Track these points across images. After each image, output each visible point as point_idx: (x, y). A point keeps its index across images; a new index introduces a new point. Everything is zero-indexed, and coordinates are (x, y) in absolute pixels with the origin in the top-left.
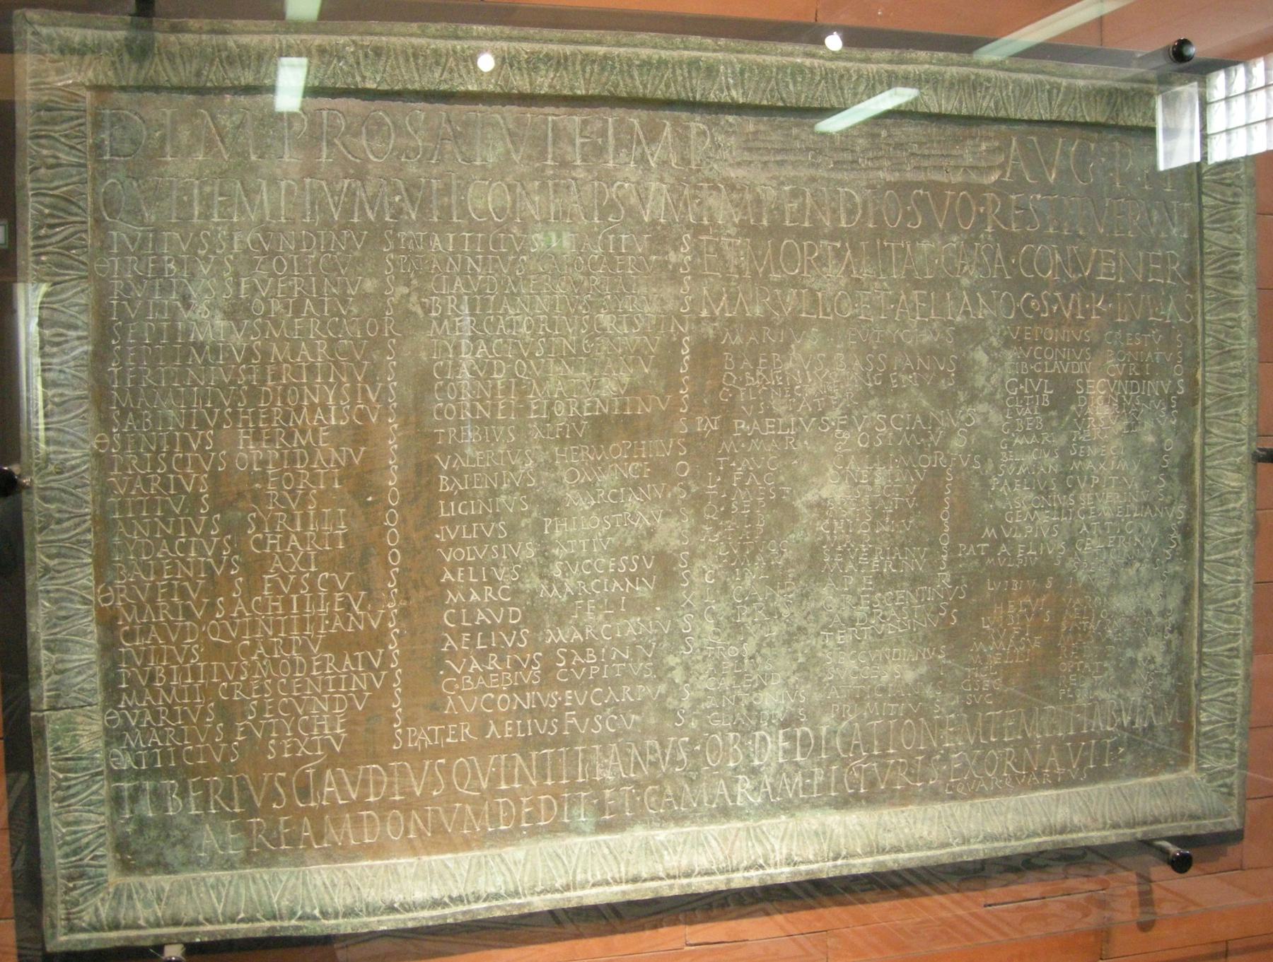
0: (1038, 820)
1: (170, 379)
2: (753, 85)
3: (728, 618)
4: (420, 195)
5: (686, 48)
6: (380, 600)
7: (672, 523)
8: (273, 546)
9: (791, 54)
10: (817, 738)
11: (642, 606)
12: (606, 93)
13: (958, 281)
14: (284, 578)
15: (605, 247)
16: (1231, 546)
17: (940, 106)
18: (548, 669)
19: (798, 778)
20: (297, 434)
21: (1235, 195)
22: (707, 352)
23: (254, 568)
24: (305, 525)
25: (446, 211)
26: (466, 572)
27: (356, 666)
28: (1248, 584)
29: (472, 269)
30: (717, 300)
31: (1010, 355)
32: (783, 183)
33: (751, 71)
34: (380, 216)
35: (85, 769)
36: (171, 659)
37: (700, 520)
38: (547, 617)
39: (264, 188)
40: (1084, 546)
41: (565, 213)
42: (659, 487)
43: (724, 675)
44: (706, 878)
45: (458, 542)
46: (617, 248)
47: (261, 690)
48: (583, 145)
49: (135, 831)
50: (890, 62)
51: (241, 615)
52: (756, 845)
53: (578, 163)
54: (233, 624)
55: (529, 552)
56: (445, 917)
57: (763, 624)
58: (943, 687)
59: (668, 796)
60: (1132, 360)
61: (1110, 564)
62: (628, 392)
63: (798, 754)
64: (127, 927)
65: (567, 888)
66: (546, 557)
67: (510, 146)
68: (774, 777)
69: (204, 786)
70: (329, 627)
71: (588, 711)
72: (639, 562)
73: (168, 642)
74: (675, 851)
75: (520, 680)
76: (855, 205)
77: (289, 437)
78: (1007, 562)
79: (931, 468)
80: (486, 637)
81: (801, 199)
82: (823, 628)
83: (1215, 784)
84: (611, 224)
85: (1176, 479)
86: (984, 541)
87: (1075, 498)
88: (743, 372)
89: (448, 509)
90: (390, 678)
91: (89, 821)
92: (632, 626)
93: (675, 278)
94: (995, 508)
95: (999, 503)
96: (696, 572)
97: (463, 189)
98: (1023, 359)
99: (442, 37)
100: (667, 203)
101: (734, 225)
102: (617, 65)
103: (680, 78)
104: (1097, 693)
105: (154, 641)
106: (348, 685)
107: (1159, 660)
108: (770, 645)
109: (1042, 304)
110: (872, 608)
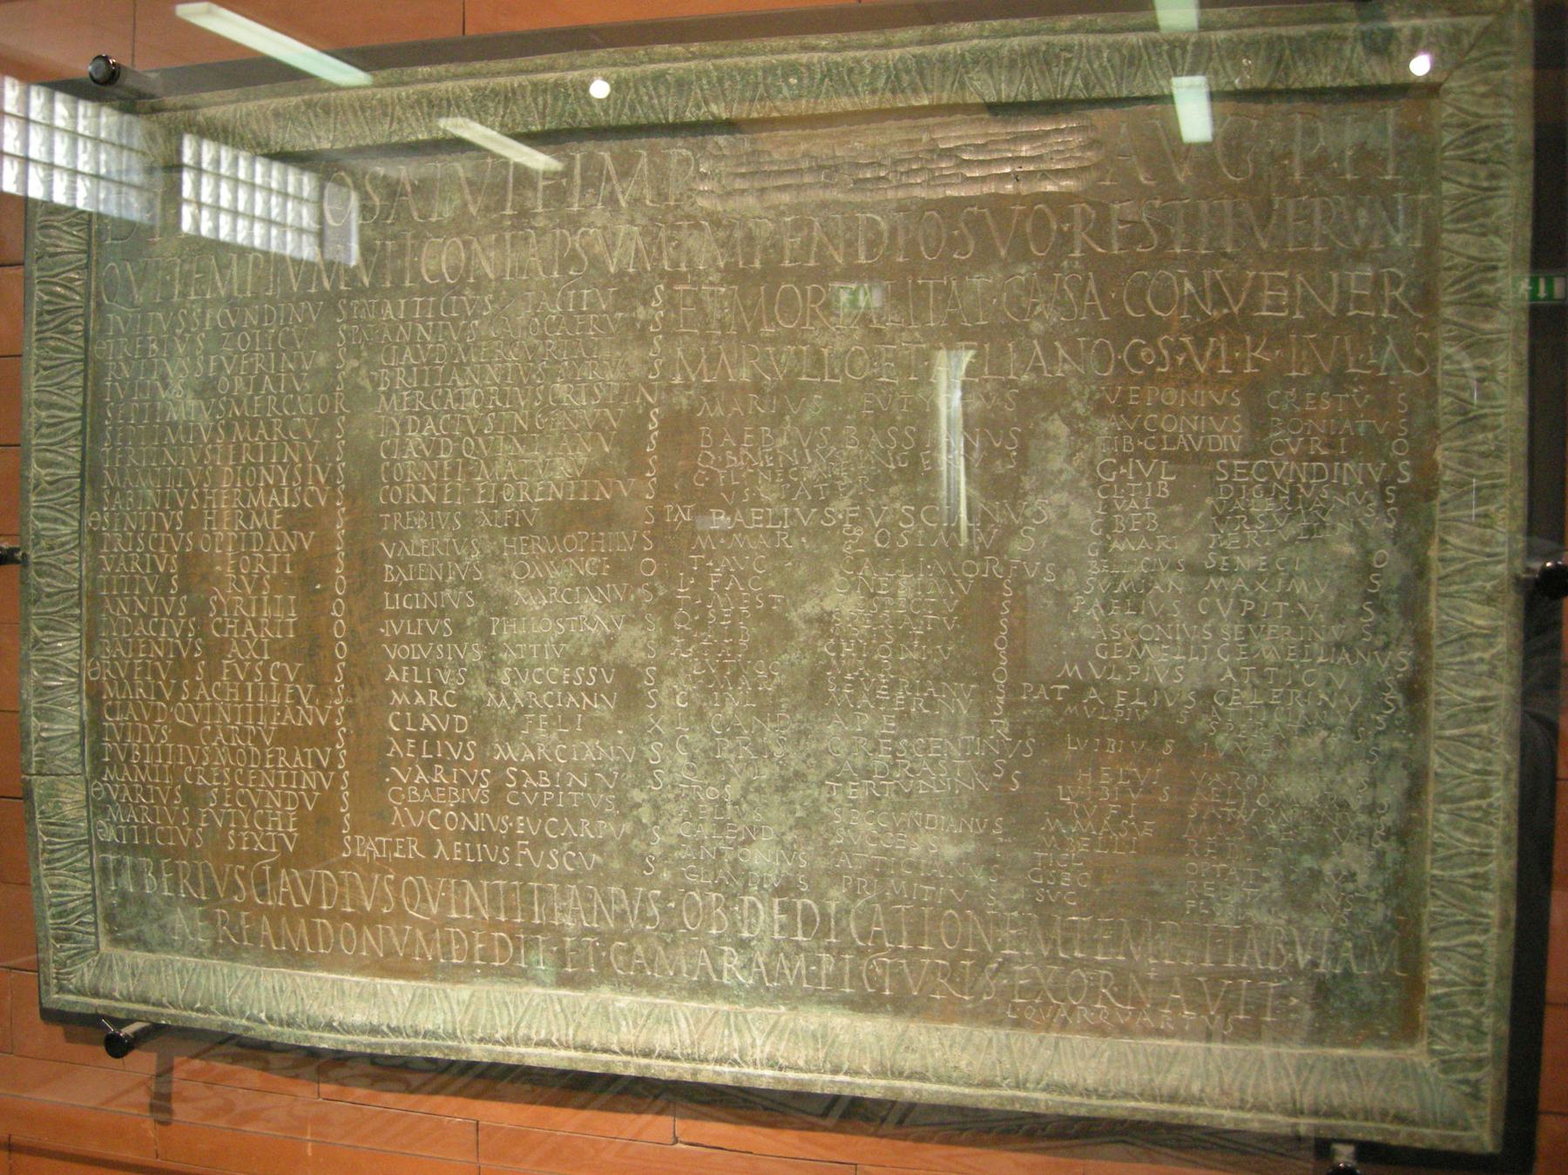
0: (1136, 1077)
1: (149, 459)
2: (737, 95)
3: (705, 751)
4: (374, 259)
5: (651, 61)
6: (327, 695)
7: (636, 632)
8: (231, 631)
9: (784, 51)
10: (825, 916)
11: (602, 728)
12: (565, 126)
13: (1026, 327)
14: (241, 663)
15: (564, 305)
16: (1476, 717)
17: (999, 92)
18: (498, 789)
19: (800, 962)
20: (254, 516)
21: (1493, 176)
22: (679, 427)
23: (215, 651)
24: (259, 610)
25: (399, 276)
26: (411, 671)
27: (305, 762)
28: (1507, 779)
29: (422, 337)
30: (694, 363)
31: (1103, 427)
32: (783, 214)
33: (732, 78)
34: (334, 285)
35: (69, 836)
36: (145, 738)
37: (669, 629)
38: (494, 730)
39: (235, 263)
40: (1227, 700)
41: (521, 269)
42: (620, 588)
43: (702, 821)
44: (669, 1063)
45: (402, 638)
46: (577, 306)
47: (221, 778)
48: (546, 187)
49: (120, 905)
50: (920, 43)
51: (203, 699)
52: (735, 1035)
53: (540, 209)
54: (196, 707)
55: (476, 655)
56: (382, 1046)
57: (749, 763)
58: (999, 872)
59: (638, 958)
60: (1315, 432)
61: (1274, 728)
62: (584, 476)
63: (800, 932)
64: (105, 997)
65: (508, 1041)
66: (493, 662)
67: (469, 197)
68: (770, 954)
69: (174, 868)
70: (280, 719)
71: (541, 843)
72: (598, 674)
73: (142, 720)
74: (635, 1024)
75: (468, 798)
76: (879, 234)
77: (247, 519)
78: (1098, 713)
79: (978, 579)
80: (432, 748)
81: (806, 231)
82: (829, 776)
83: (1454, 1077)
84: (572, 278)
85: (1394, 611)
86: (1063, 680)
87: (1213, 630)
88: (724, 450)
89: (392, 602)
90: (338, 780)
91: (75, 888)
92: (590, 750)
93: (643, 338)
94: (1080, 637)
95: (1085, 631)
96: (665, 692)
97: (417, 251)
98: (1126, 431)
99: (390, 85)
100: (637, 251)
101: (718, 270)
102: (571, 91)
103: (646, 99)
104: (1252, 913)
105: (131, 719)
106: (299, 783)
107: (1363, 877)
108: (759, 790)
109: (1159, 354)
110: (895, 757)
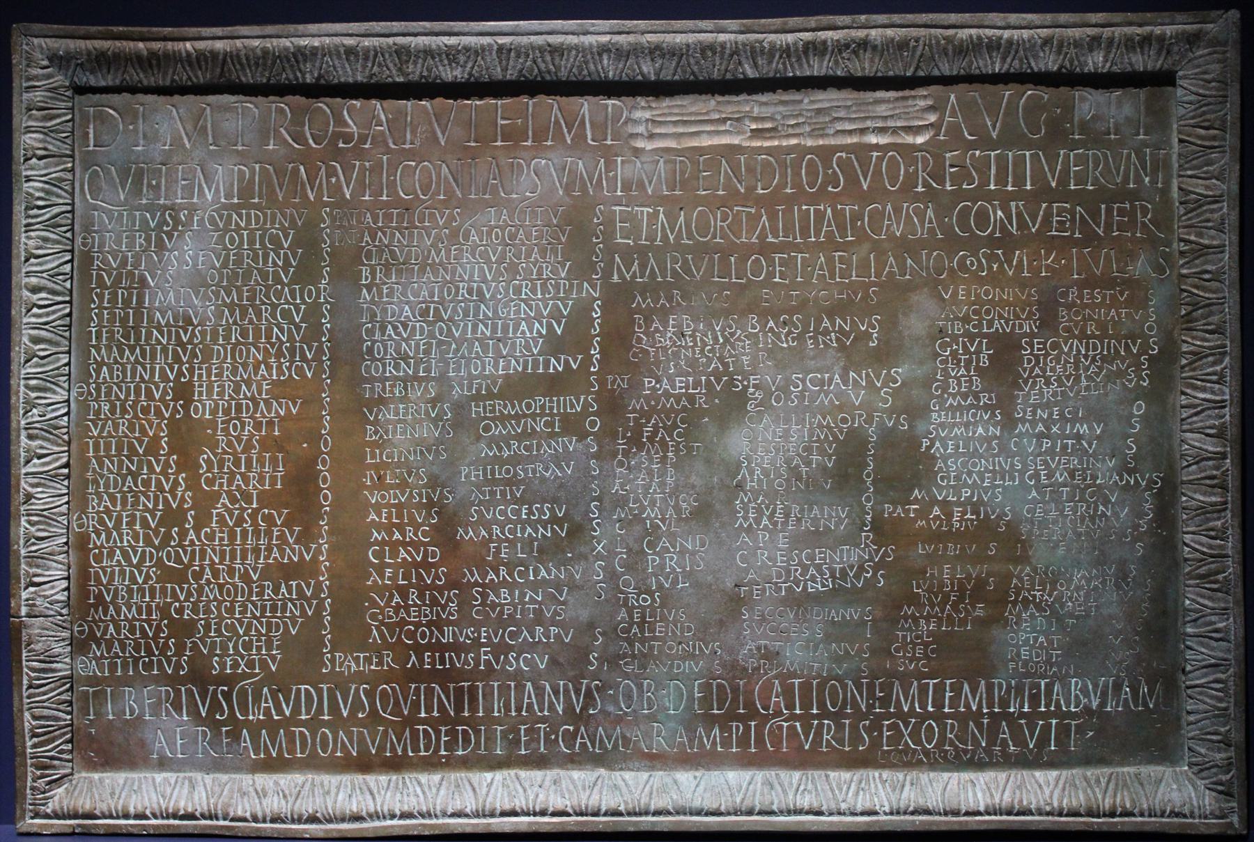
47: (207, 611)
70: (267, 558)
75: (438, 615)
89: (373, 457)
109: (979, 261)
